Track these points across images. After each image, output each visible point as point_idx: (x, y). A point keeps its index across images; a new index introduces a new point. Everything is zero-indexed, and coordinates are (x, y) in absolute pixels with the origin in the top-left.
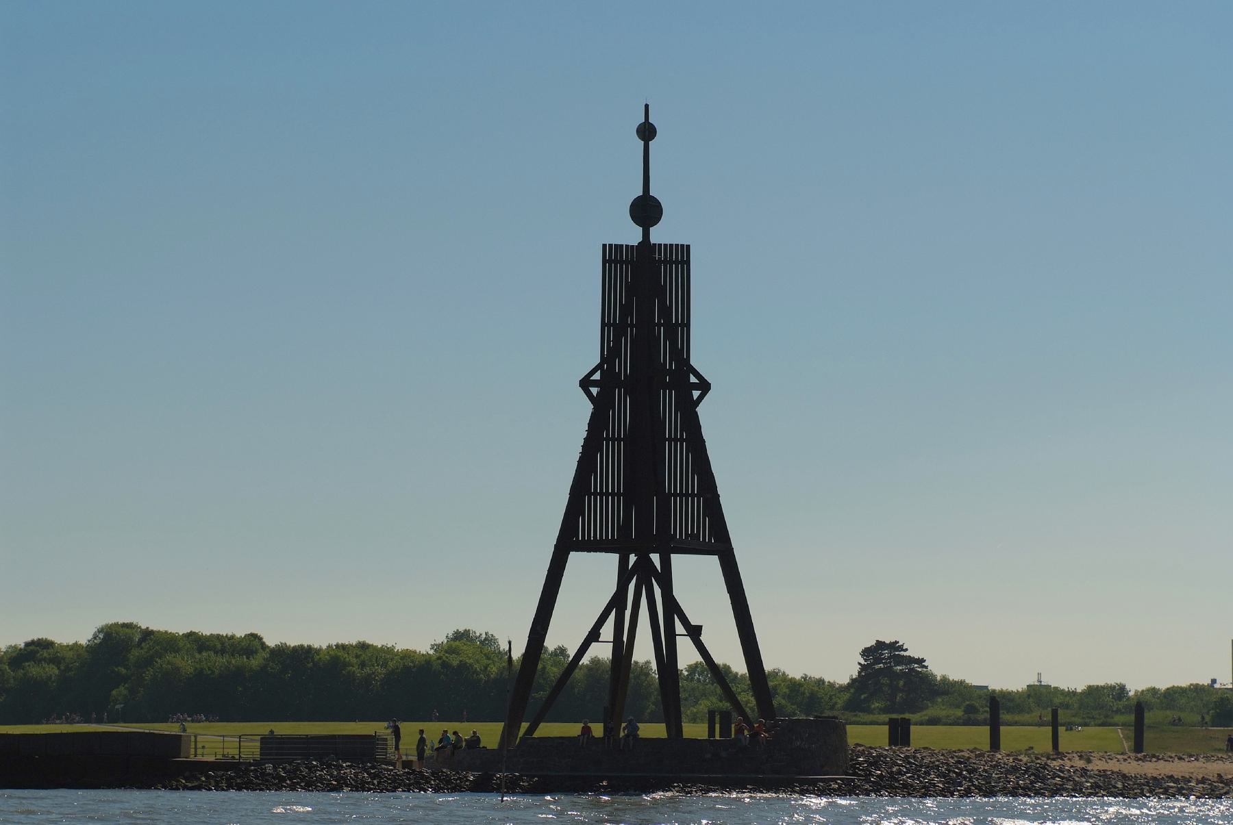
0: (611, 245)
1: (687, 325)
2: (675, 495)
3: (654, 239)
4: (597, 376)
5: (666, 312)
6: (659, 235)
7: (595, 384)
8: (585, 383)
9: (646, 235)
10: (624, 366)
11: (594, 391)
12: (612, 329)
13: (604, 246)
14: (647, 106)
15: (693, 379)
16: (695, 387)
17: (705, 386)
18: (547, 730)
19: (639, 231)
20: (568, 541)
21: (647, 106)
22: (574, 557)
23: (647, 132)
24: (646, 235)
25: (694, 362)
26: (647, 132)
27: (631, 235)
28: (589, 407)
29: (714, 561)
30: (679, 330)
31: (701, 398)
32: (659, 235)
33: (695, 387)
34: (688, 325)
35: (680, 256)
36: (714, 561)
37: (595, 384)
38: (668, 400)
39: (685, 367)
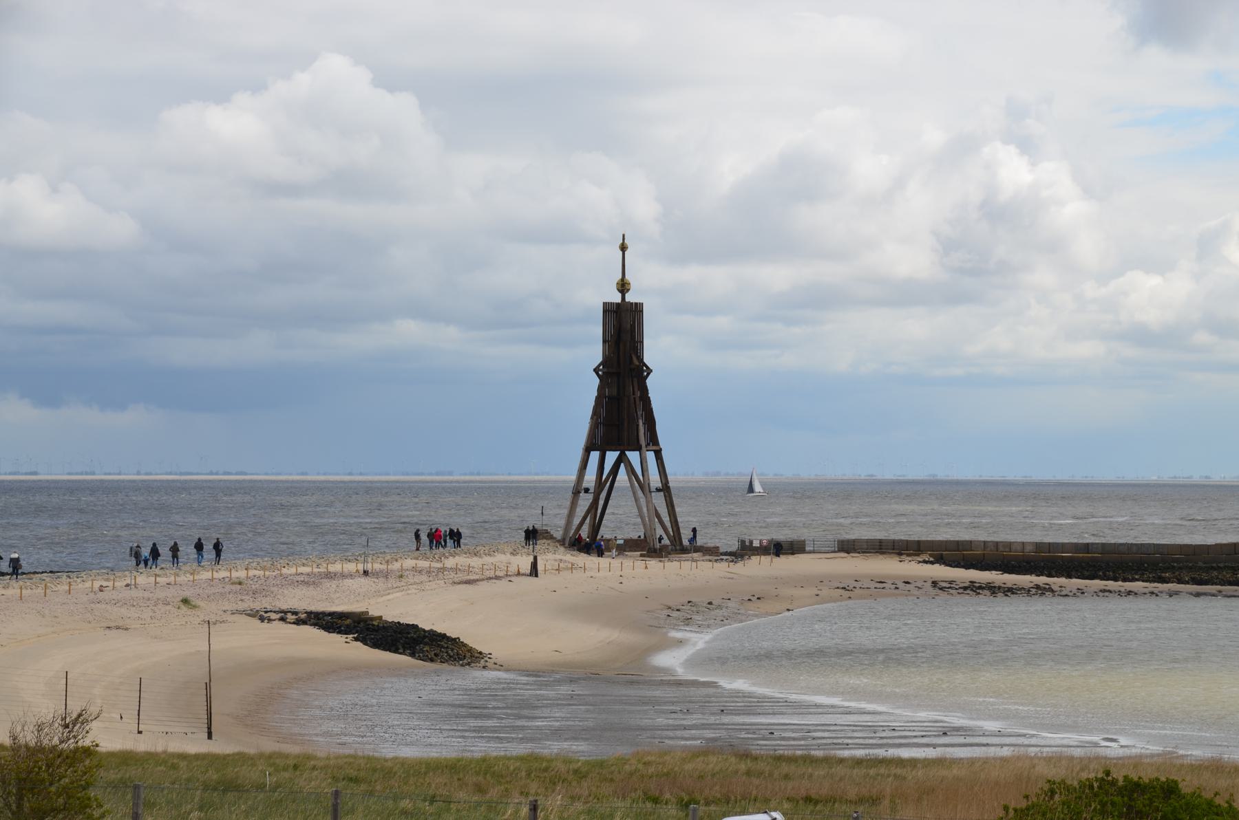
3: (627, 300)
6: (630, 298)
7: (601, 370)
8: (596, 370)
9: (623, 298)
14: (624, 236)
15: (645, 368)
21: (624, 236)
23: (623, 248)
24: (623, 298)
25: (645, 360)
26: (623, 248)
27: (617, 298)
35: (637, 309)
37: (601, 370)
39: (641, 360)
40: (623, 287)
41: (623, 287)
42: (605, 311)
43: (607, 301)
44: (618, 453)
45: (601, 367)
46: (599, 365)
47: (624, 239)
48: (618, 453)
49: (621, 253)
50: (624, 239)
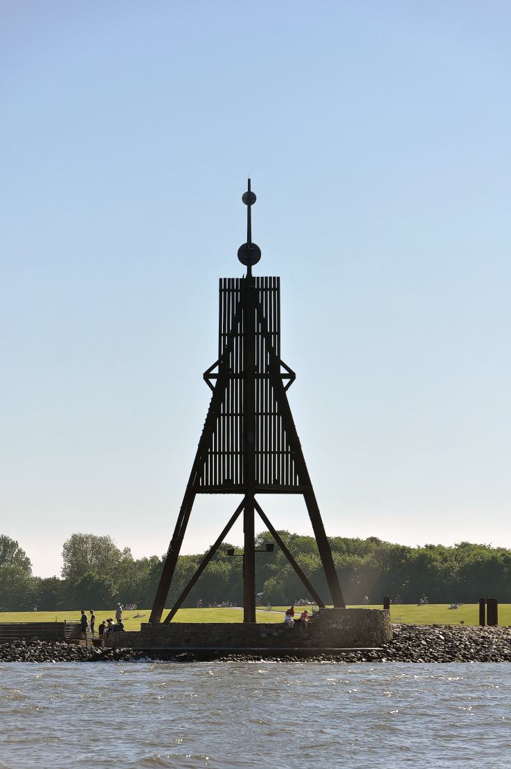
0: (225, 279)
1: (278, 334)
2: (262, 452)
4: (216, 371)
5: (263, 321)
6: (258, 271)
7: (214, 376)
10: (237, 365)
11: (214, 382)
12: (227, 337)
13: (221, 280)
14: (249, 180)
16: (285, 376)
17: (292, 376)
18: (184, 616)
19: (245, 267)
20: (195, 487)
21: (249, 180)
22: (199, 498)
23: (249, 198)
25: (282, 358)
26: (249, 198)
27: (239, 271)
28: (210, 394)
29: (299, 499)
30: (272, 336)
32: (258, 271)
33: (285, 376)
34: (279, 333)
35: (273, 285)
36: (299, 499)
37: (214, 376)
38: (263, 388)
39: (276, 362)
40: (249, 254)
41: (249, 254)
44: (240, 498)
48: (240, 498)
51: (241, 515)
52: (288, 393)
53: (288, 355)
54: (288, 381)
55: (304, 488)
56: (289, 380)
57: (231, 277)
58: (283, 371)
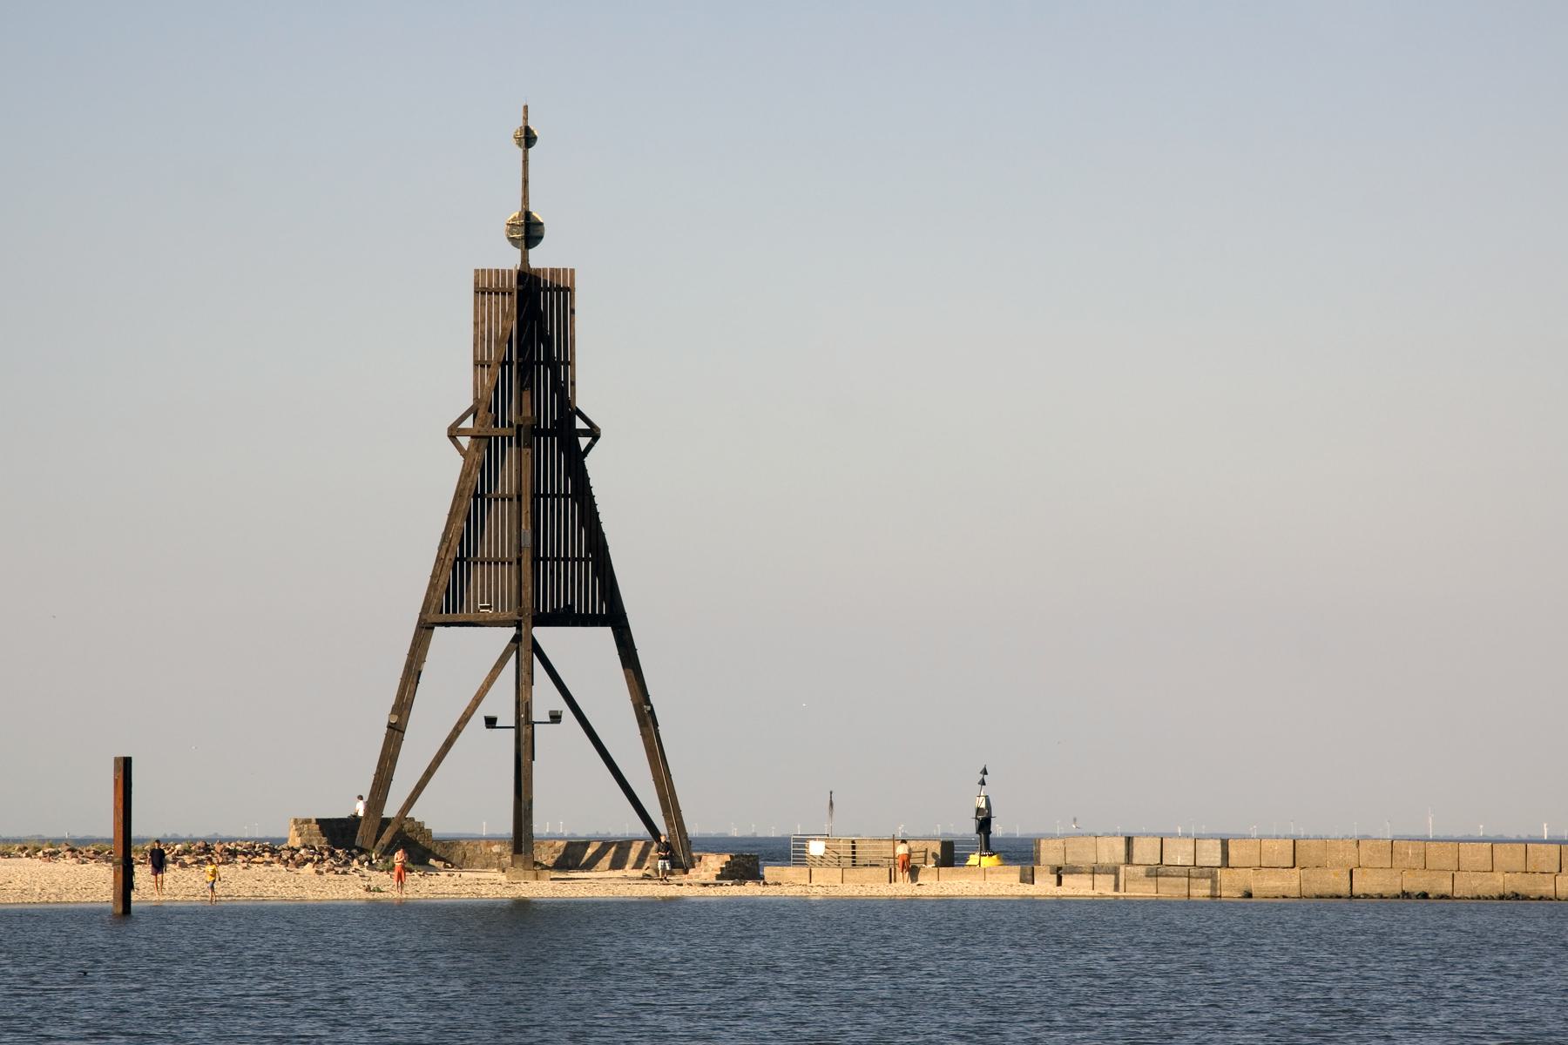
1: (569, 363)
4: (468, 423)
6: (540, 258)
7: (464, 432)
9: (525, 260)
13: (476, 271)
14: (526, 108)
16: (585, 433)
17: (594, 433)
19: (518, 253)
21: (526, 108)
23: (528, 139)
24: (525, 260)
25: (581, 403)
26: (528, 138)
27: (509, 259)
29: (606, 633)
31: (590, 447)
33: (585, 433)
36: (606, 633)
37: (464, 432)
39: (568, 411)
40: (529, 232)
41: (529, 232)
42: (480, 291)
43: (480, 268)
44: (512, 631)
45: (468, 423)
46: (463, 418)
47: (526, 119)
48: (512, 631)
49: (520, 151)
50: (526, 119)
51: (512, 662)
52: (588, 461)
53: (587, 397)
54: (588, 440)
55: (615, 618)
56: (588, 440)
57: (497, 268)
58: (580, 424)
